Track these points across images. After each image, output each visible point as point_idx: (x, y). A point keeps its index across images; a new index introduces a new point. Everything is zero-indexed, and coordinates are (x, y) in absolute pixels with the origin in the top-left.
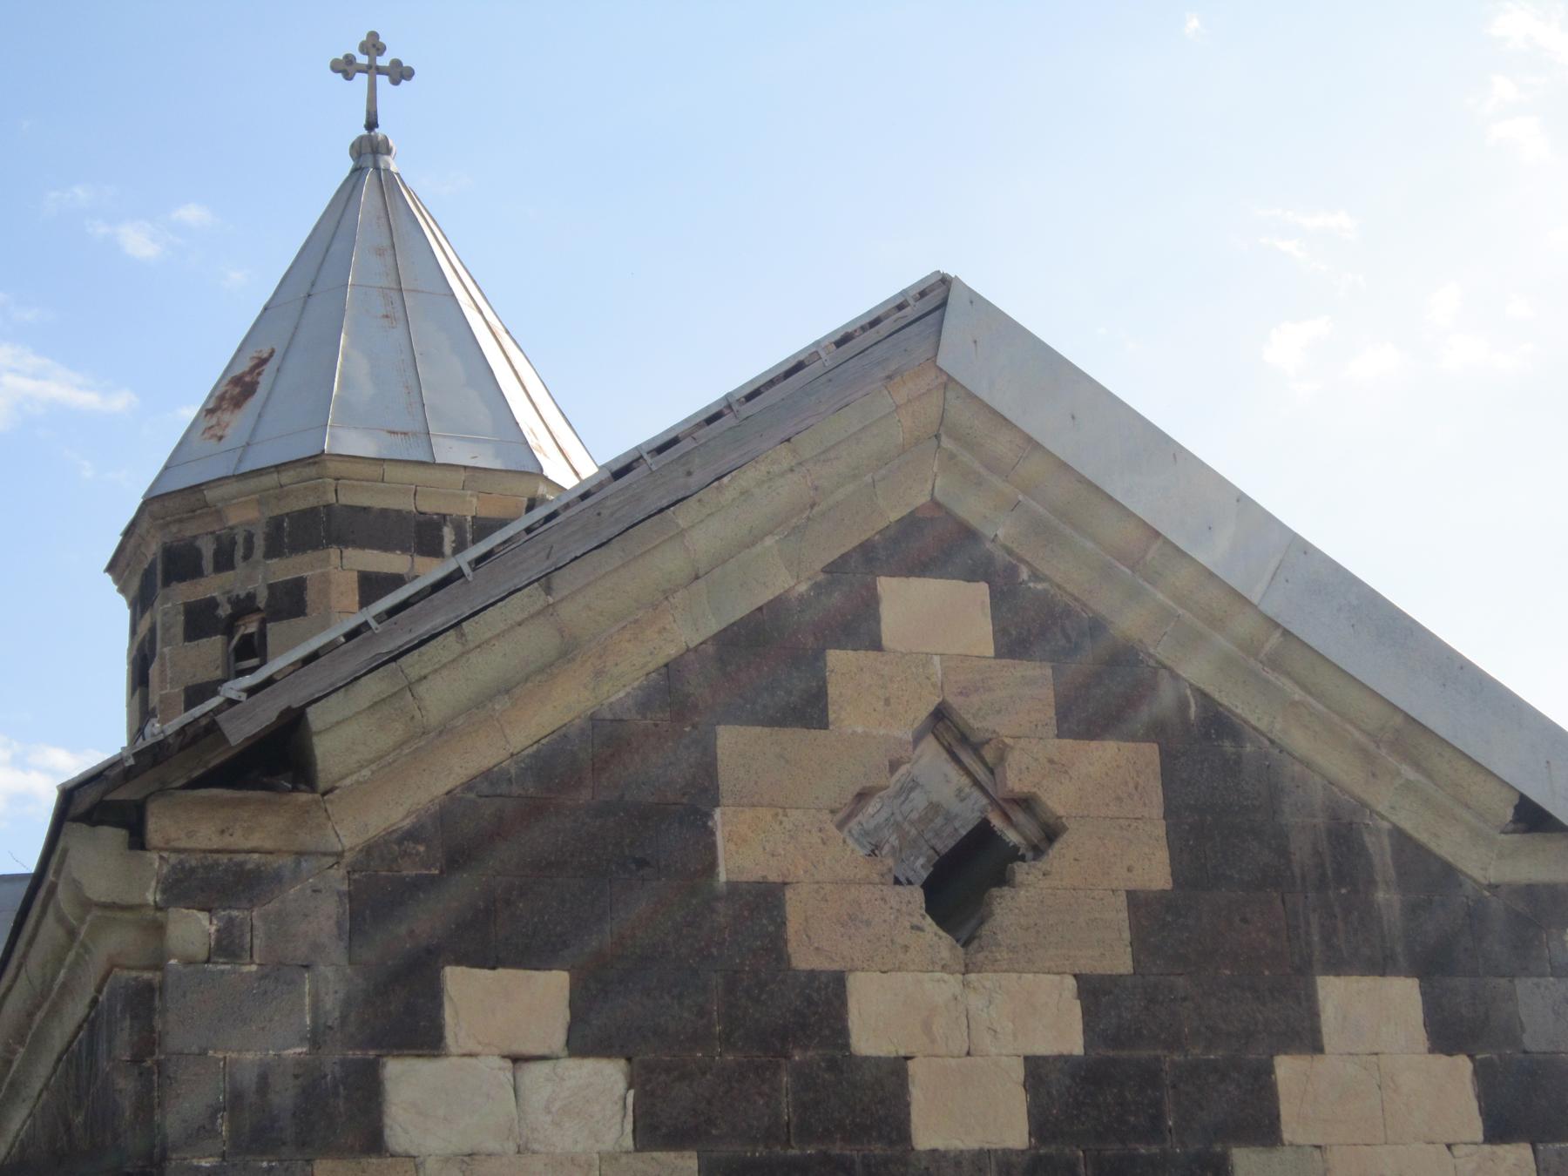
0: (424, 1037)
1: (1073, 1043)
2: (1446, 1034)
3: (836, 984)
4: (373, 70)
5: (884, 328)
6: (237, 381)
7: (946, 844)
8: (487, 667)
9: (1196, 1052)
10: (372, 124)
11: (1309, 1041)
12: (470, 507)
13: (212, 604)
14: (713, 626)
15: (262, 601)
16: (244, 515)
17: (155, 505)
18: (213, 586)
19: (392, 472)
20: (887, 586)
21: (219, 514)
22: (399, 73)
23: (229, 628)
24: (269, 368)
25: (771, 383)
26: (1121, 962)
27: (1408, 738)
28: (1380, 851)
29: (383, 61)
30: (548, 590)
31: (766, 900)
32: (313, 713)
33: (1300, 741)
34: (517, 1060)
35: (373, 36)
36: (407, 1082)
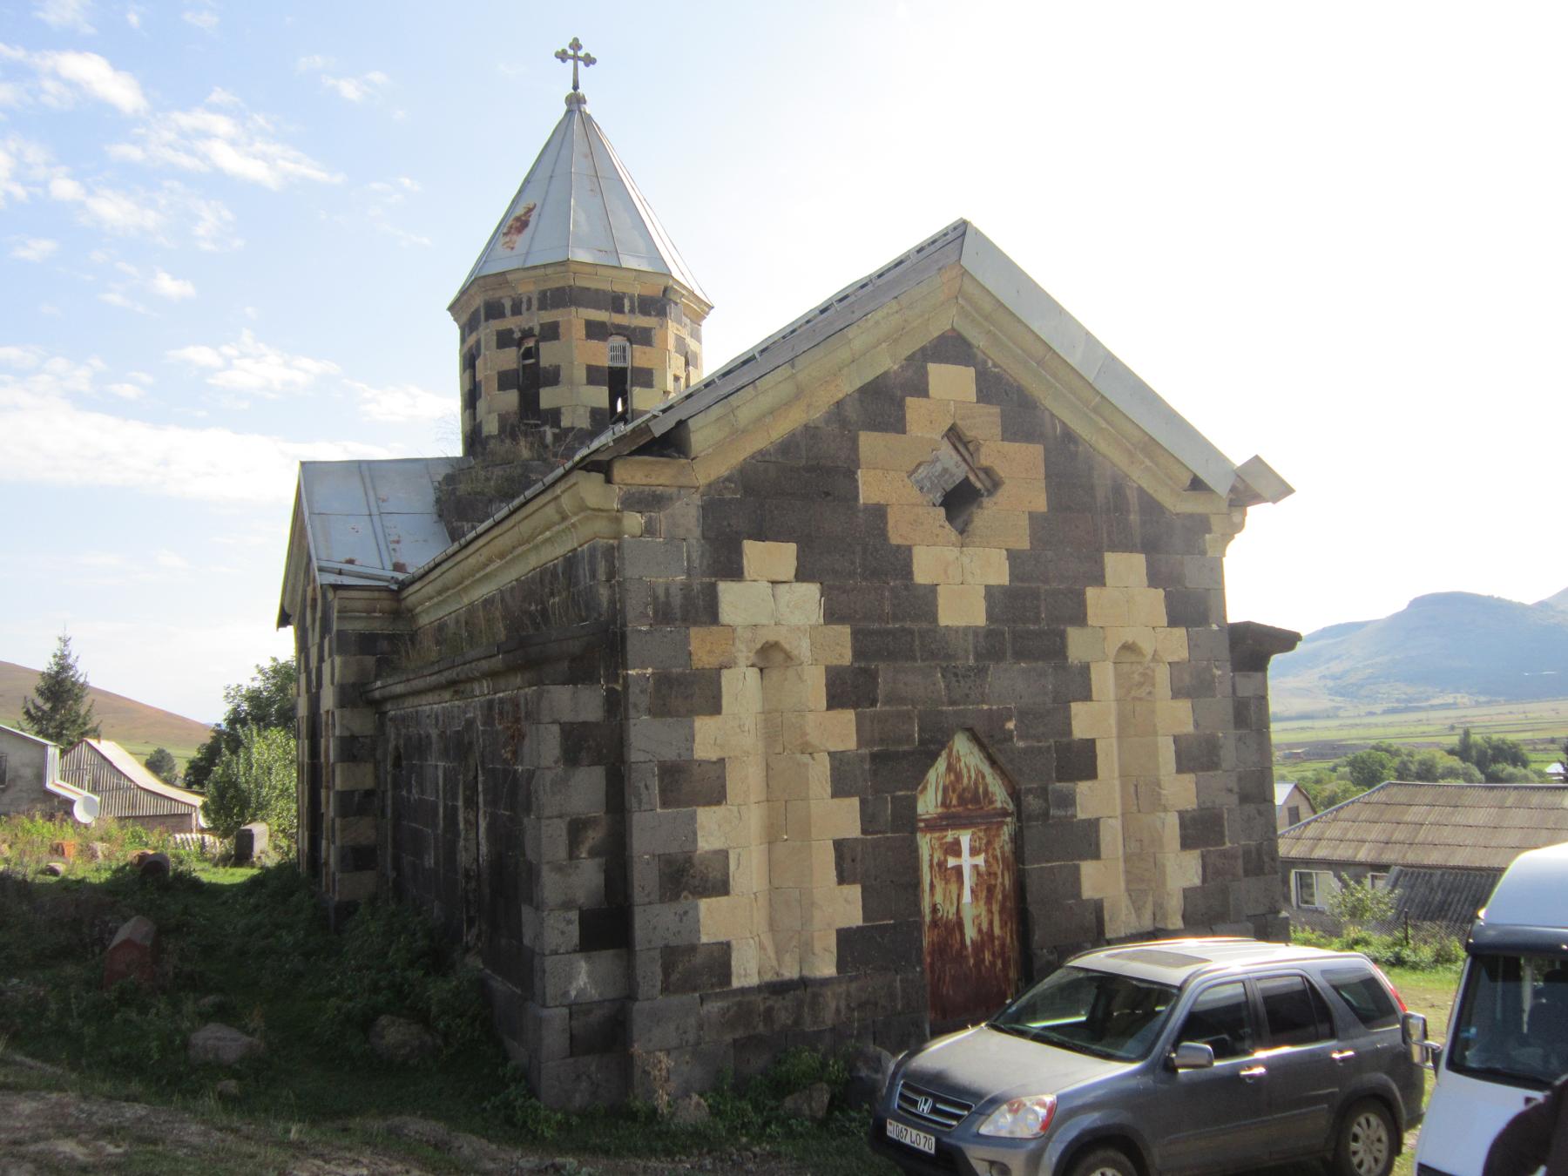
0: (735, 572)
1: (1005, 580)
2: (1154, 579)
4: (576, 58)
5: (938, 245)
6: (518, 219)
7: (949, 487)
8: (765, 402)
9: (1055, 585)
10: (576, 87)
11: (1100, 580)
12: (637, 290)
13: (510, 331)
14: (858, 384)
15: (537, 331)
16: (528, 289)
17: (478, 282)
18: (510, 323)
19: (600, 271)
22: (589, 61)
23: (519, 344)
24: (535, 213)
25: (889, 270)
26: (1025, 544)
27: (1150, 446)
29: (581, 54)
30: (793, 366)
31: (879, 513)
32: (690, 422)
33: (1103, 446)
35: (576, 40)
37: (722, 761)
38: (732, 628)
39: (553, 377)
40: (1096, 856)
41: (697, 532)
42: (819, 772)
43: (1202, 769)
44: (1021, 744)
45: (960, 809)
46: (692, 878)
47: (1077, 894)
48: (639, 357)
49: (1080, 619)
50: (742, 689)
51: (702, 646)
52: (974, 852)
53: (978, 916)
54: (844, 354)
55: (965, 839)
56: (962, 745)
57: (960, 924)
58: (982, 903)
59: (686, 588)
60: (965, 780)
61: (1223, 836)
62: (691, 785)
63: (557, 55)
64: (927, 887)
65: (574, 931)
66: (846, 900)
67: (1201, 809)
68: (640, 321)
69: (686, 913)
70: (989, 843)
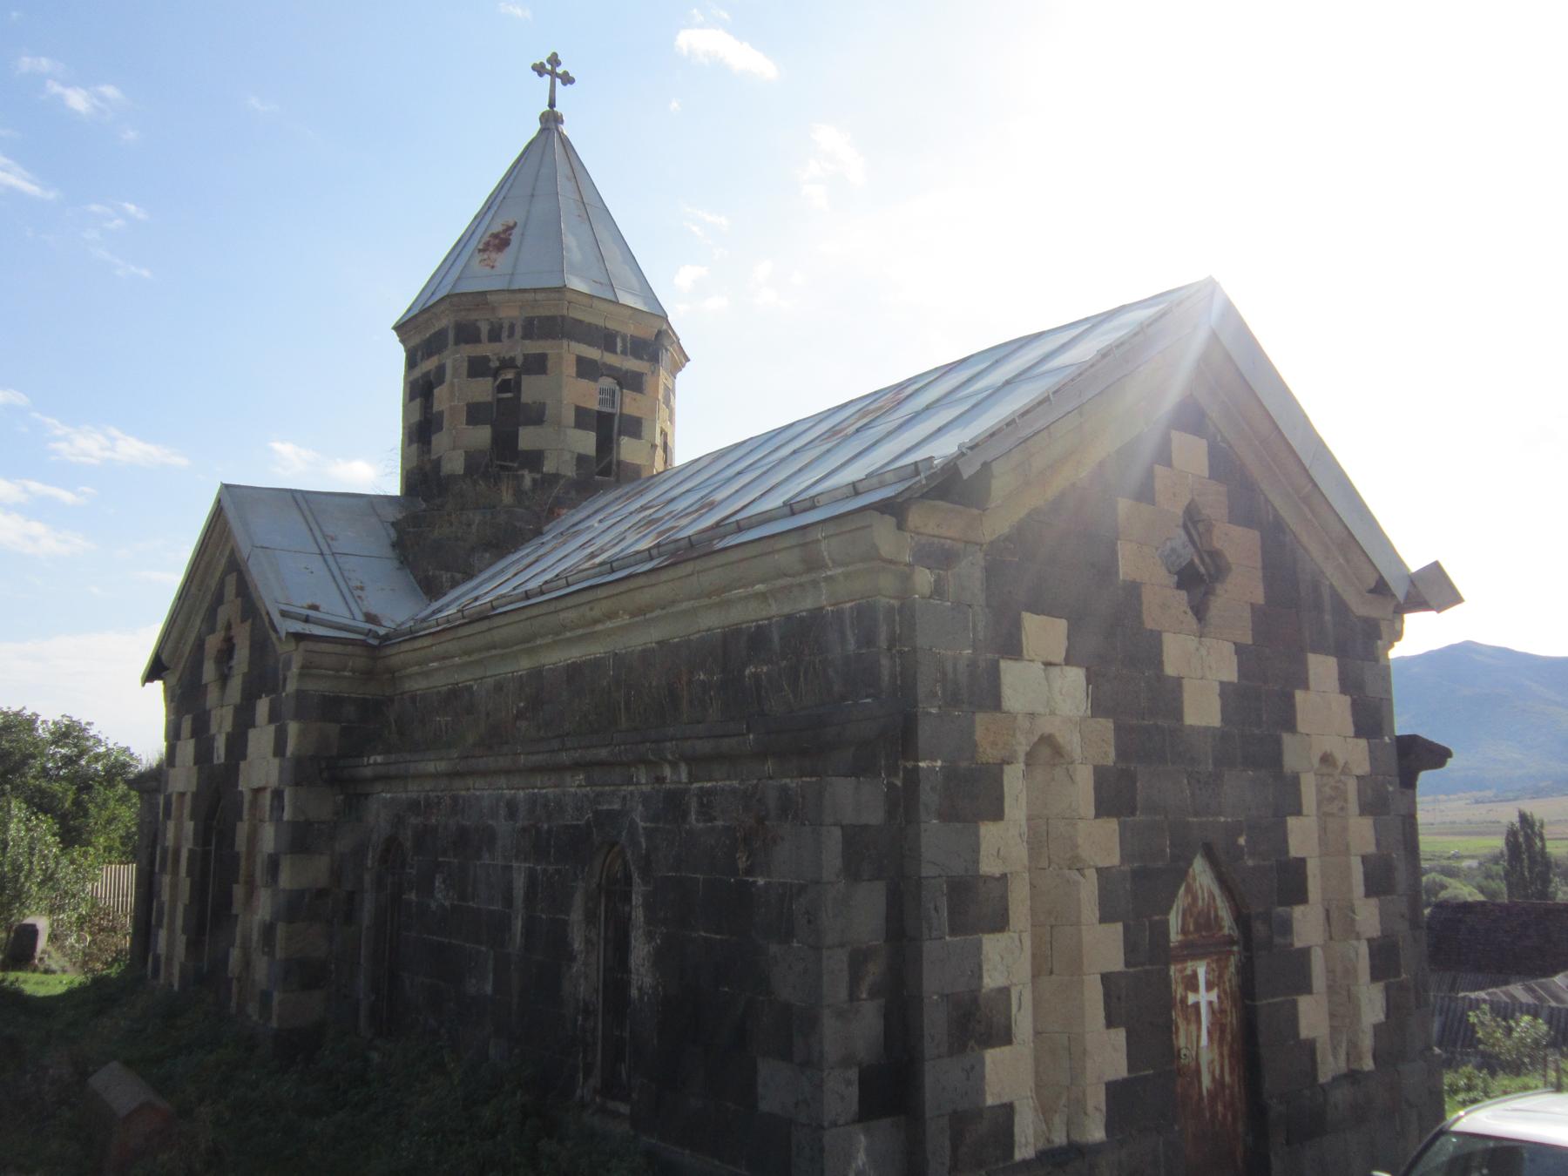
0: (1013, 650)
4: (553, 74)
6: (495, 236)
10: (552, 104)
12: (630, 329)
13: (486, 359)
15: (519, 362)
16: (509, 313)
18: (486, 349)
19: (596, 302)
21: (493, 309)
22: (567, 79)
23: (495, 374)
24: (516, 232)
26: (1248, 640)
29: (559, 70)
34: (1048, 664)
37: (1004, 876)
38: (1012, 716)
39: (537, 416)
44: (1250, 863)
46: (979, 1024)
47: (1297, 1034)
48: (631, 404)
53: (1212, 1062)
57: (1198, 1071)
59: (972, 664)
62: (978, 906)
63: (535, 68)
65: (854, 1092)
68: (631, 364)
69: (973, 1067)
70: (1220, 976)
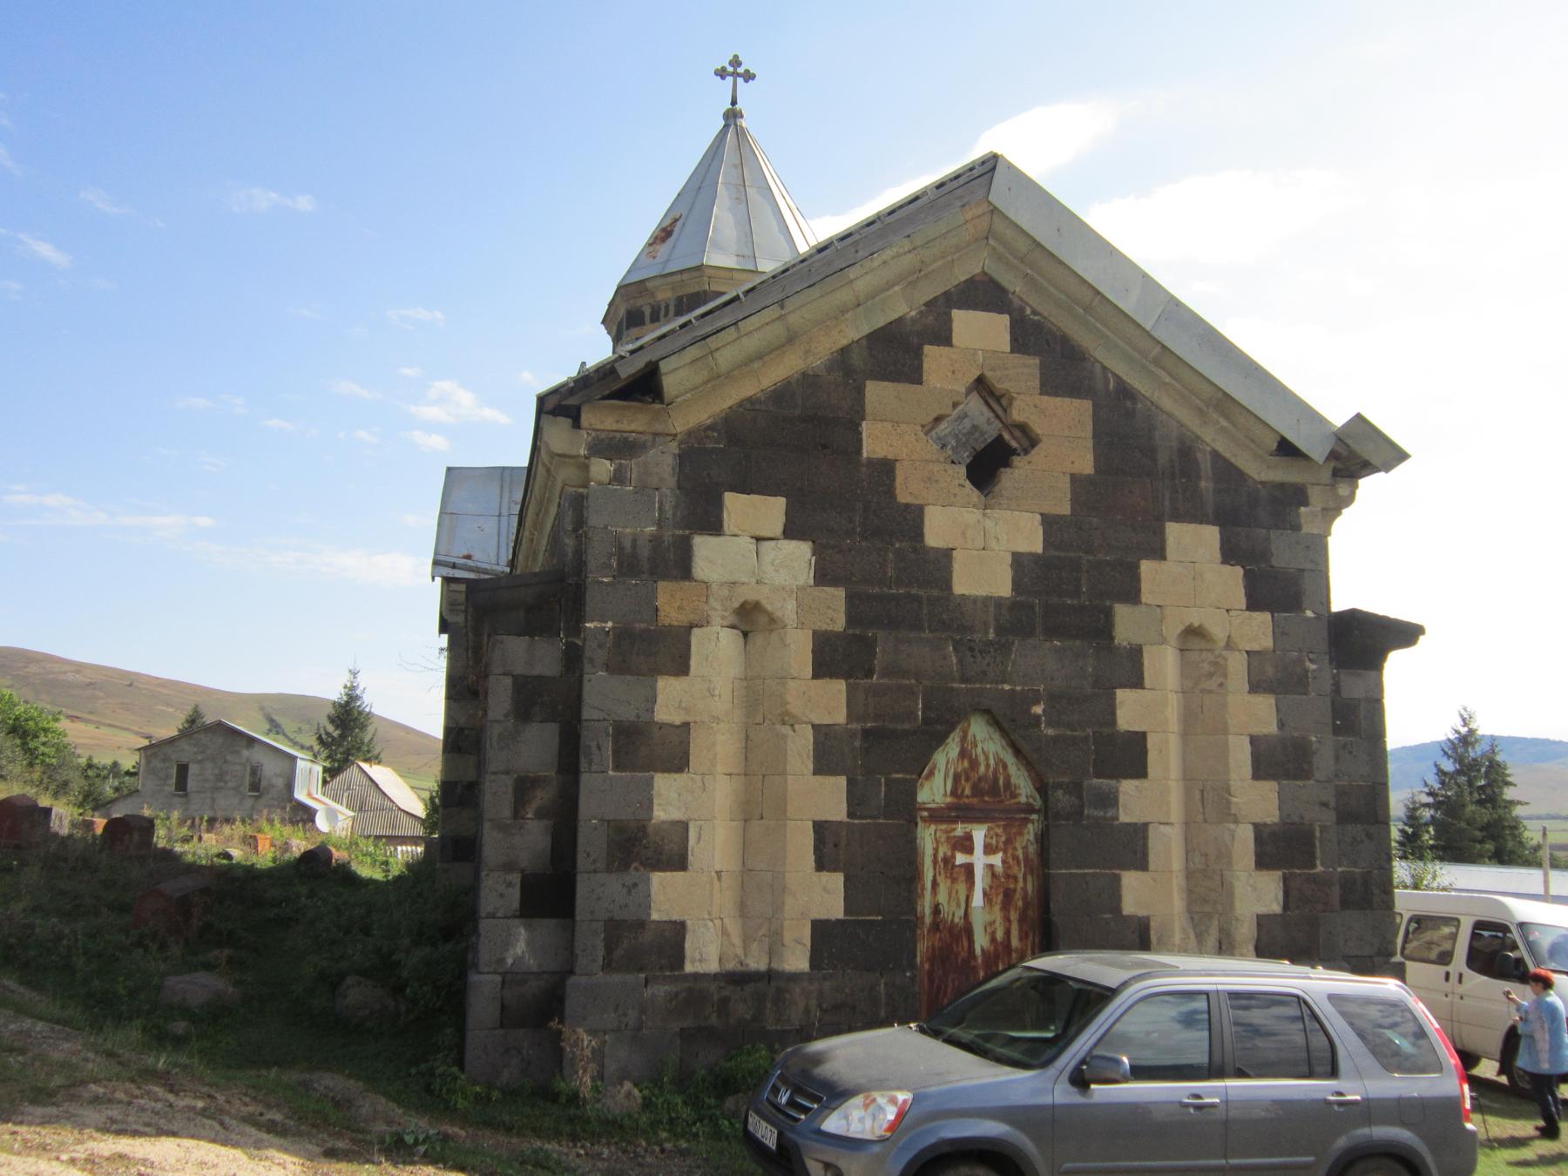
0: (714, 526)
1: (1038, 548)
2: (1230, 554)
3: (920, 510)
4: (735, 75)
5: (962, 180)
6: (664, 230)
7: (980, 446)
8: (751, 344)
9: (1100, 556)
10: (734, 103)
11: (1159, 553)
14: (866, 330)
16: (664, 295)
17: (623, 290)
19: (735, 275)
20: (957, 315)
21: (653, 295)
22: (748, 77)
24: (679, 224)
25: (901, 207)
26: (1065, 509)
27: (1224, 403)
28: (1206, 465)
29: (741, 70)
30: (782, 307)
31: (886, 468)
32: (662, 364)
33: (1167, 403)
34: (758, 539)
35: (736, 57)
36: (705, 548)
37: (686, 725)
38: (707, 585)
40: (1143, 865)
41: (672, 481)
42: (801, 744)
43: (1288, 776)
44: (1050, 732)
45: (975, 800)
47: (1117, 909)
49: (1132, 595)
50: (717, 650)
51: (671, 603)
52: (989, 850)
54: (844, 296)
55: (979, 834)
56: (979, 729)
57: (968, 930)
58: (997, 908)
59: (656, 540)
60: (982, 769)
61: (1312, 856)
63: (717, 73)
64: (928, 885)
65: (516, 893)
66: (825, 889)
67: (1283, 822)
69: (635, 885)
70: (1008, 842)
